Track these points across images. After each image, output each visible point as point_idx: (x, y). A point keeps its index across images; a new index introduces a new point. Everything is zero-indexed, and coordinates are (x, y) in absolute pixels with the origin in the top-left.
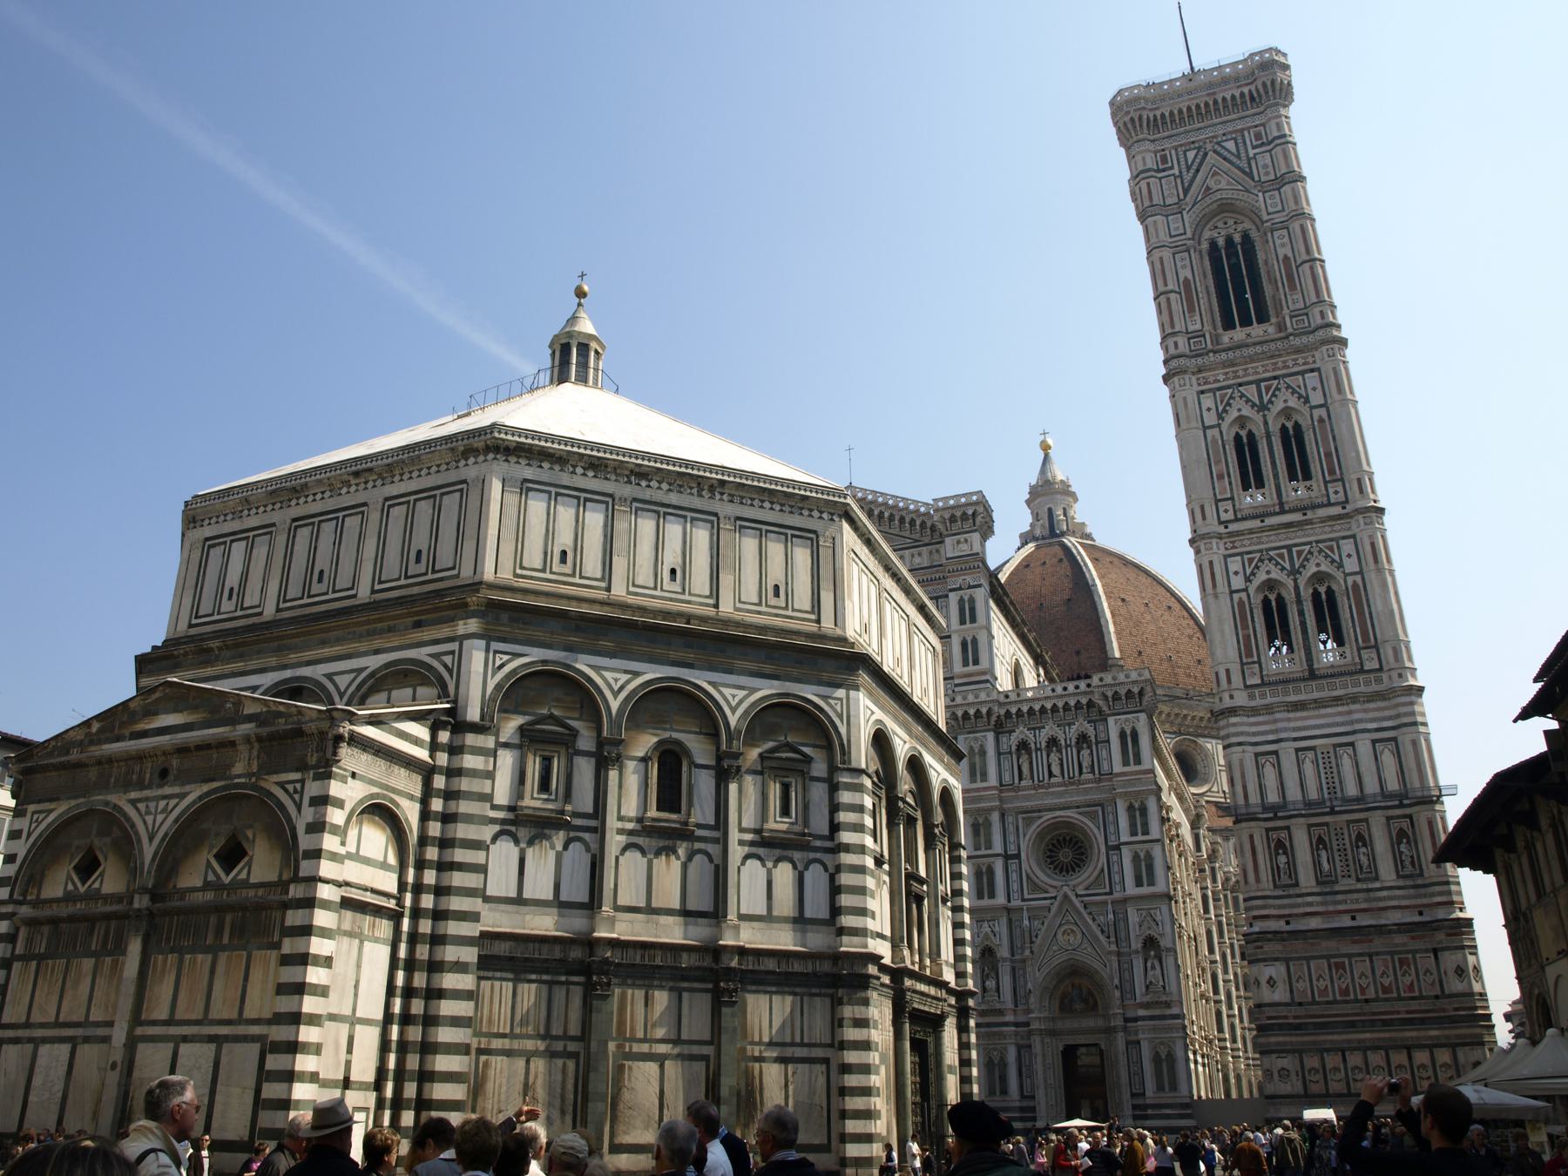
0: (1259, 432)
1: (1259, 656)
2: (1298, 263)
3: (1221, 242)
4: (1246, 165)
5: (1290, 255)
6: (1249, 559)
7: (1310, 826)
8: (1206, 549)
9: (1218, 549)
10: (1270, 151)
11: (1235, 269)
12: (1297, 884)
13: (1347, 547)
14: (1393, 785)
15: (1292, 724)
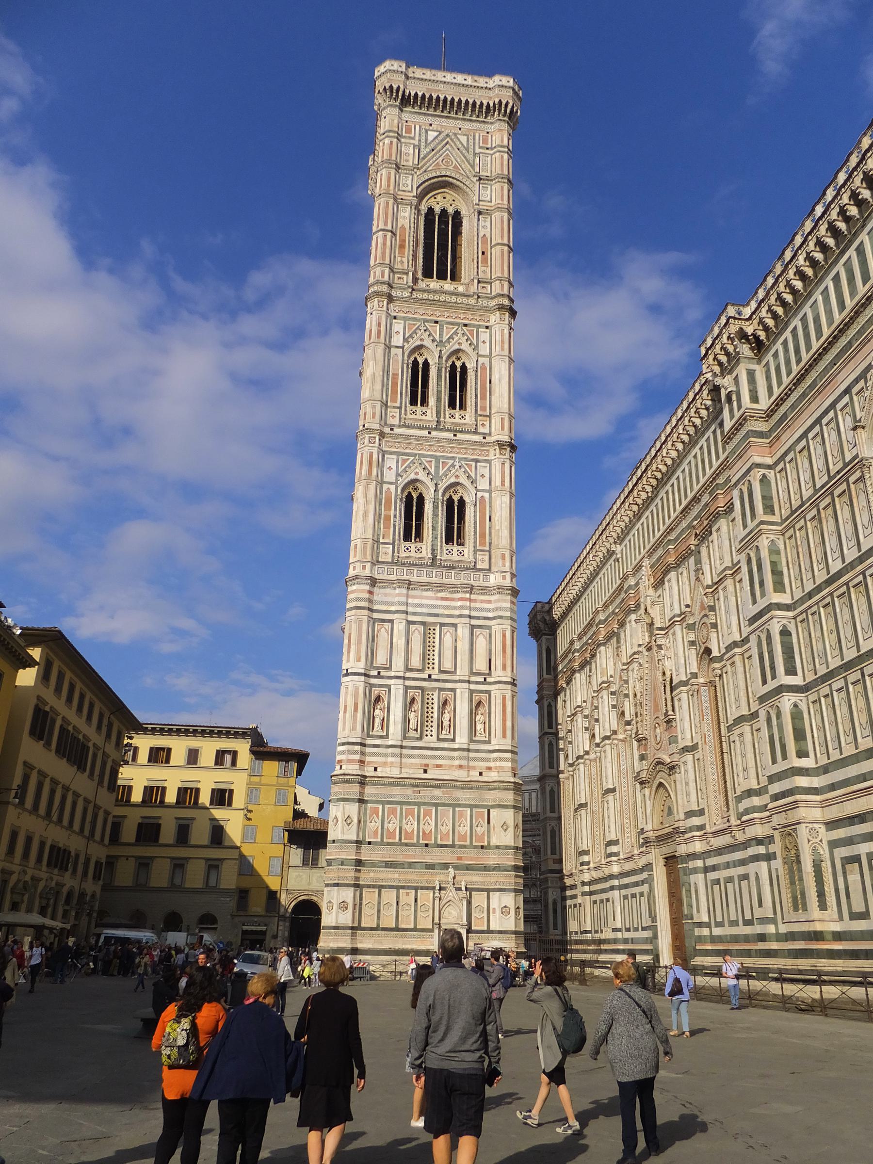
0: (433, 362)
1: (394, 538)
2: (493, 243)
3: (437, 210)
4: (471, 159)
5: (488, 236)
6: (403, 459)
7: (407, 688)
8: (370, 442)
9: (380, 445)
10: (492, 155)
11: (443, 234)
12: (386, 737)
13: (483, 469)
14: (481, 665)
15: (410, 601)
